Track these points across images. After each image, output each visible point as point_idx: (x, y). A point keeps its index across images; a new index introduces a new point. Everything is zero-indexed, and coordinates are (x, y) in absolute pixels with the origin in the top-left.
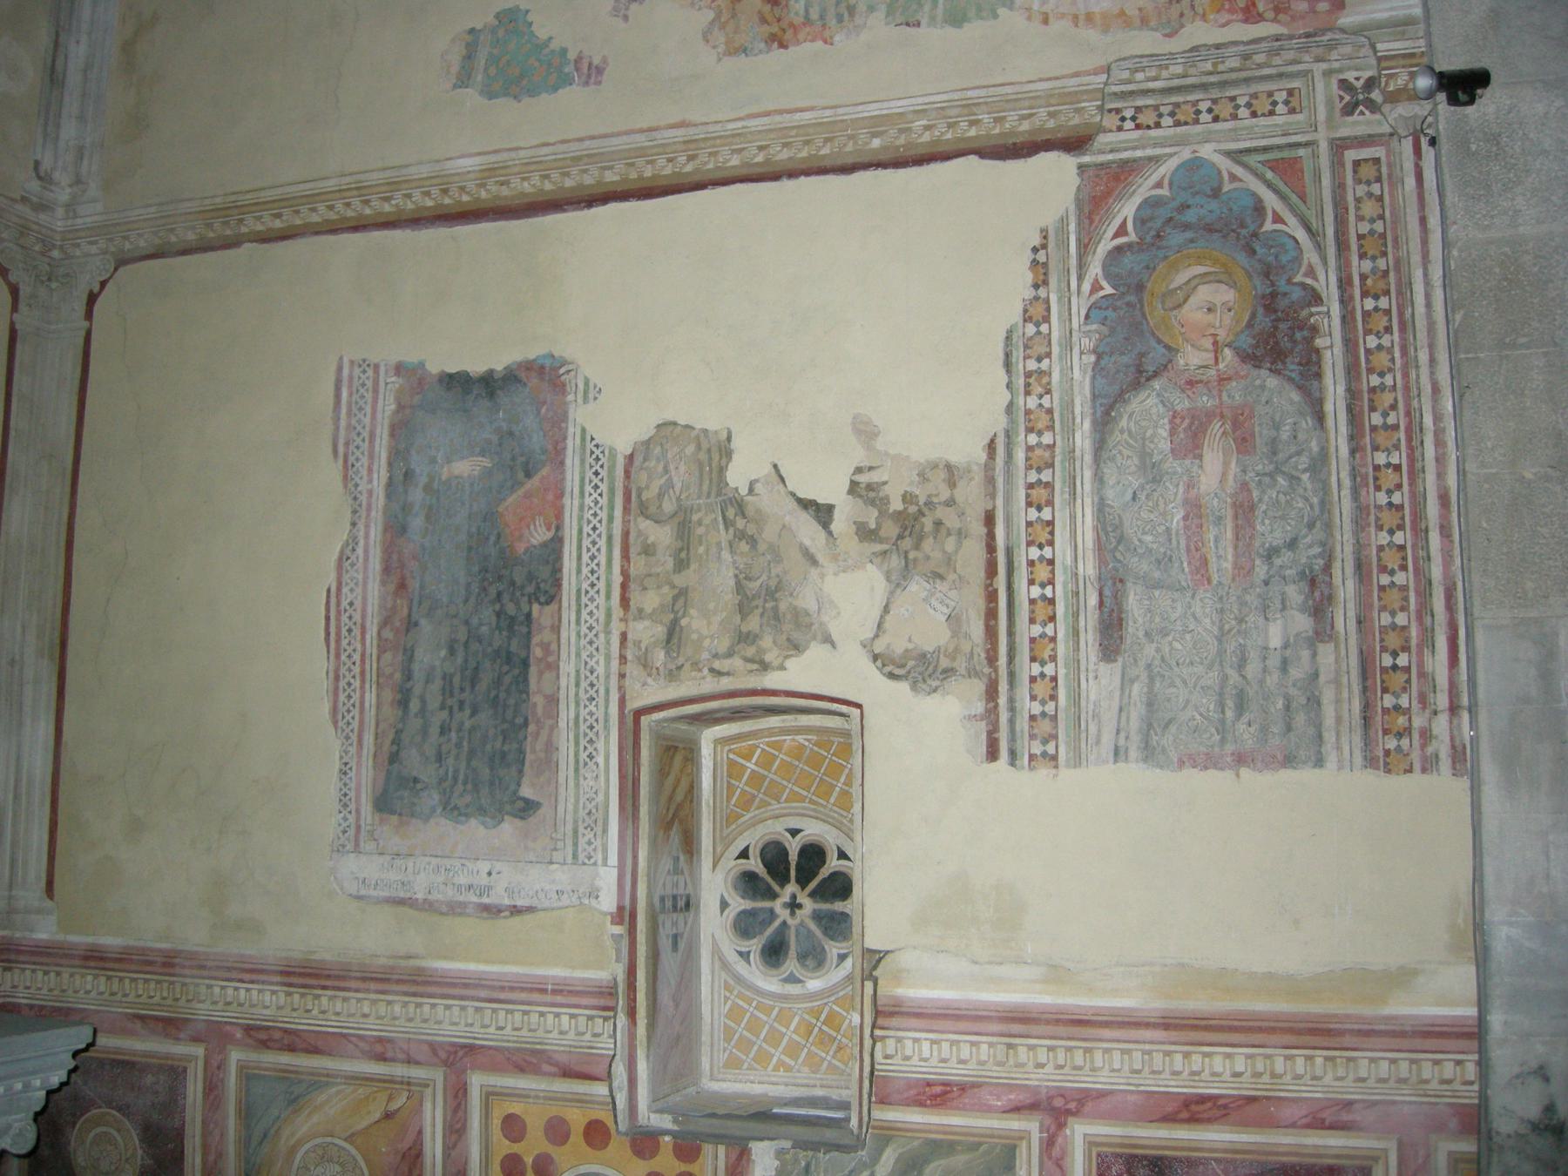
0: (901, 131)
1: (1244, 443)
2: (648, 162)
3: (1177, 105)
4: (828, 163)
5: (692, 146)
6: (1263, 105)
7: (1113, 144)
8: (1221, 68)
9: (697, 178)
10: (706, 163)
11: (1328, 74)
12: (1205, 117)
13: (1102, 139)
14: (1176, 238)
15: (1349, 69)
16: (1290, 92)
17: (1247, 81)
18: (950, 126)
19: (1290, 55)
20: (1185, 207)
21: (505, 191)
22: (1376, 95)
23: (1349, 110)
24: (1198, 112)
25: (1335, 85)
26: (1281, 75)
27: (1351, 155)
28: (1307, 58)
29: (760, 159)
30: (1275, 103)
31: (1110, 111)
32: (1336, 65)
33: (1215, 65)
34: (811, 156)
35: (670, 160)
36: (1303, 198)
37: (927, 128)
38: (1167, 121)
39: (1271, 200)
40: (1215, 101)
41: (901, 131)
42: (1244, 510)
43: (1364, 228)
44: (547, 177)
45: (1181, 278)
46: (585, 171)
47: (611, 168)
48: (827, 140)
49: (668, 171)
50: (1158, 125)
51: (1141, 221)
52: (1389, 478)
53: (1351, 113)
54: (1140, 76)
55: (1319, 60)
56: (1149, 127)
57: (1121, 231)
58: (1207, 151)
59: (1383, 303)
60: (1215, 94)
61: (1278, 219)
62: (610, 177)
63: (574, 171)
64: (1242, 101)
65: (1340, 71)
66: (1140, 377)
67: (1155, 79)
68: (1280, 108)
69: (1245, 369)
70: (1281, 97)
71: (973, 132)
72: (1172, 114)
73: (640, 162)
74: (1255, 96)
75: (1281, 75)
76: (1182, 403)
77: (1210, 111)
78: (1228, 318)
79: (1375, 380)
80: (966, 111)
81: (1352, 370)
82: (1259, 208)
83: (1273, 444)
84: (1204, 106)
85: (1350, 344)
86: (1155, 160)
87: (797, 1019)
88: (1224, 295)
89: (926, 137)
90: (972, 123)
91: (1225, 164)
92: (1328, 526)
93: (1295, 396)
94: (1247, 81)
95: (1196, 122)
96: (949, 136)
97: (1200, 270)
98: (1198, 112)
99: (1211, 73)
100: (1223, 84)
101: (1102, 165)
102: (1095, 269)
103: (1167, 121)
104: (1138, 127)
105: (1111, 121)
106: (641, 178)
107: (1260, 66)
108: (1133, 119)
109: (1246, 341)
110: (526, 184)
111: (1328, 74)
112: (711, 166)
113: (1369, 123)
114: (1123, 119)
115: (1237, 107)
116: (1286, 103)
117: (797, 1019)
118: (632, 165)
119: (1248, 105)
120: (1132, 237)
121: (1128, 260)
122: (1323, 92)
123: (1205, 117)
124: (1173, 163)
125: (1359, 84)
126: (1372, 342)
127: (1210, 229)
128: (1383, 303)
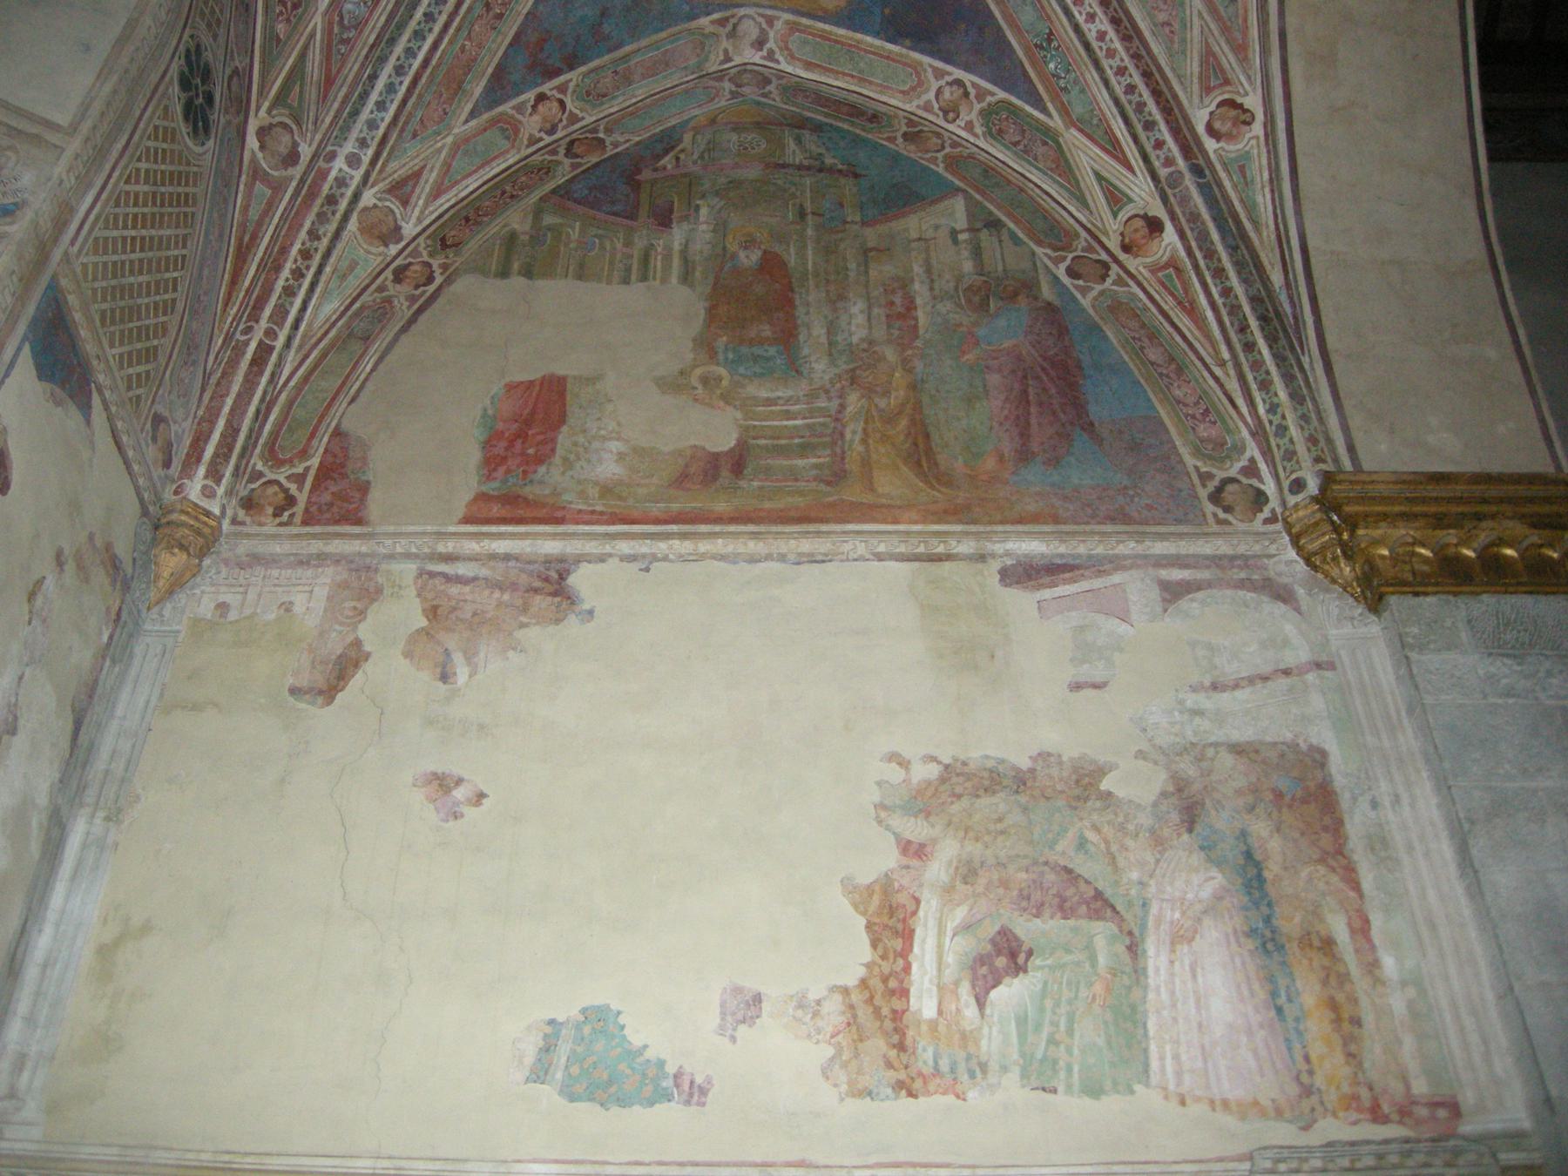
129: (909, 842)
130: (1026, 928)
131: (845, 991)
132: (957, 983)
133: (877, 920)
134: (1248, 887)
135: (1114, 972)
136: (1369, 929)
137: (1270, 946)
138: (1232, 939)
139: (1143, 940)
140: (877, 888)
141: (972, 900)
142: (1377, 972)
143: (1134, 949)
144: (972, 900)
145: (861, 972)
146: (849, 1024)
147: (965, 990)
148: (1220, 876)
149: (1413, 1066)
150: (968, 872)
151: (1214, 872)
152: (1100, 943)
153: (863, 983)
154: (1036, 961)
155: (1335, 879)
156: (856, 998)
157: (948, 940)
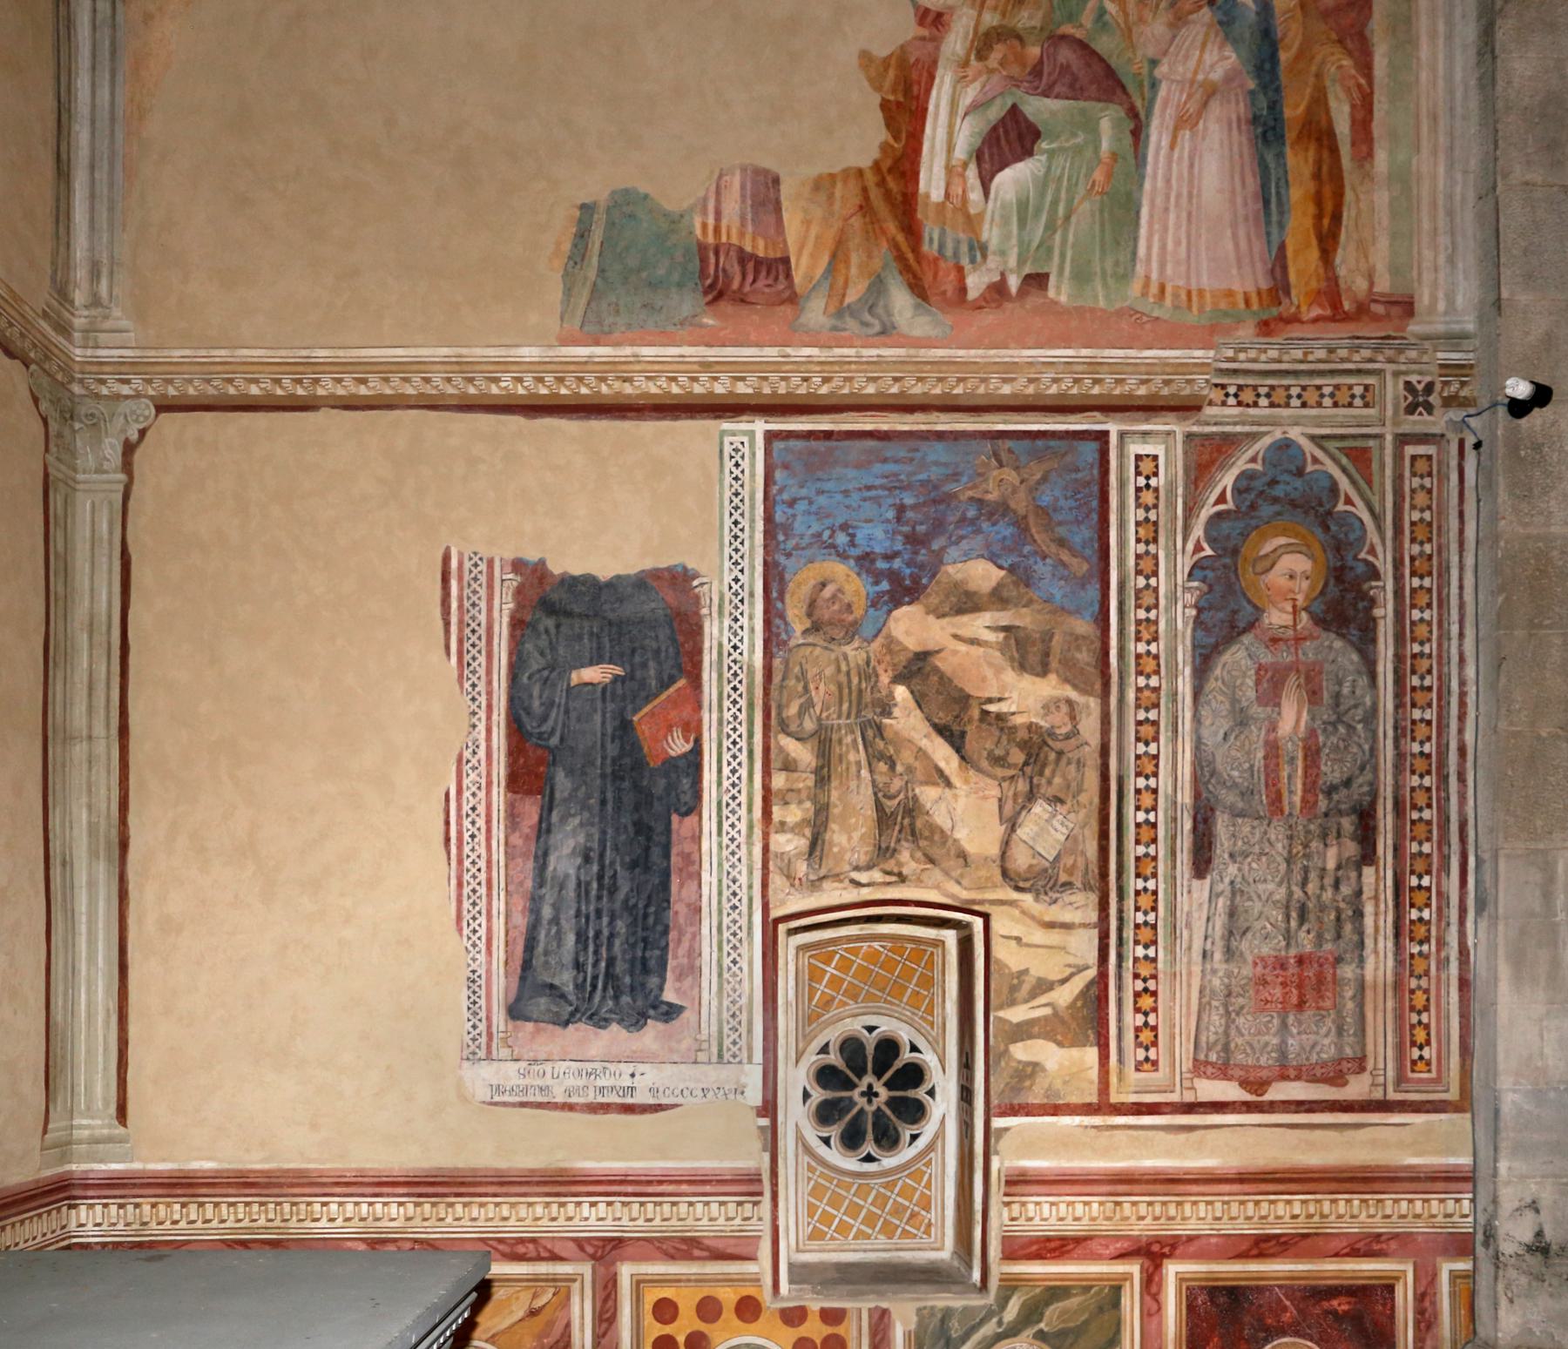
0: (1031, 381)
1: (1314, 696)
2: (783, 379)
3: (1272, 388)
4: (962, 402)
5: (827, 368)
6: (1343, 397)
7: (1221, 416)
8: (1310, 358)
9: (833, 401)
10: (841, 387)
11: (1396, 374)
12: (1295, 402)
13: (1209, 411)
14: (1266, 510)
15: (1413, 372)
16: (1367, 388)
17: (1332, 372)
18: (1076, 381)
19: (1366, 353)
20: (1273, 483)
21: (628, 389)
22: (1434, 399)
23: (1411, 409)
24: (1289, 397)
25: (1401, 386)
26: (1359, 372)
27: (1410, 450)
28: (1381, 358)
29: (894, 390)
30: (1353, 396)
31: (1216, 385)
32: (1403, 367)
33: (1305, 354)
34: (945, 394)
35: (805, 379)
36: (1369, 483)
37: (1055, 381)
38: (1263, 402)
39: (1344, 484)
40: (1304, 388)
41: (1031, 381)
42: (1312, 755)
43: (1416, 516)
44: (674, 379)
45: (1268, 548)
46: (716, 379)
47: (743, 379)
48: (960, 380)
49: (802, 391)
50: (1256, 404)
51: (1238, 491)
52: (1422, 730)
53: (1412, 413)
54: (1242, 356)
55: (1390, 361)
56: (1248, 405)
57: (1221, 499)
58: (1295, 433)
59: (1427, 582)
60: (1305, 381)
61: (1349, 501)
62: (742, 388)
63: (704, 377)
64: (1327, 390)
65: (1405, 373)
66: (1233, 631)
67: (1254, 361)
68: (1358, 402)
69: (1317, 631)
70: (1358, 390)
71: (1096, 390)
72: (1268, 396)
73: (774, 377)
74: (1337, 387)
75: (1359, 372)
76: (1266, 658)
77: (1299, 396)
78: (1305, 584)
79: (1416, 648)
80: (1091, 368)
81: (1399, 639)
82: (1334, 489)
83: (1337, 696)
84: (1295, 391)
85: (1399, 615)
86: (1254, 437)
87: (874, 1193)
88: (1300, 563)
89: (1054, 390)
90: (1096, 381)
91: (1308, 447)
92: (1375, 770)
93: (1355, 657)
94: (1332, 372)
95: (1288, 405)
96: (1075, 391)
97: (1282, 540)
98: (1289, 397)
99: (1302, 362)
100: (1311, 373)
101: (1208, 436)
102: (1198, 531)
103: (1263, 402)
104: (1239, 404)
105: (1217, 395)
106: (774, 394)
107: (1343, 360)
108: (1236, 395)
109: (1318, 608)
110: (651, 384)
111: (1396, 374)
112: (846, 391)
113: (1425, 423)
114: (1227, 395)
115: (1322, 396)
116: (1363, 397)
117: (874, 1193)
118: (766, 379)
119: (1332, 395)
120: (1230, 505)
121: (1226, 526)
122: (1393, 390)
123: (1295, 402)
124: (1267, 441)
125: (1420, 387)
126: (1416, 615)
127: (1293, 504)
128: (1427, 582)
129: (927, 11)
130: (1037, 108)
131: (860, 172)
132: (965, 165)
133: (891, 98)
134: (1259, 70)
135: (1114, 156)
136: (1371, 120)
137: (1270, 135)
138: (1234, 125)
139: (1148, 125)
140: (893, 62)
141: (984, 78)
142: (1367, 166)
143: (1138, 133)
144: (984, 78)
145: (875, 154)
146: (861, 207)
147: (972, 173)
148: (1234, 56)
149: (1381, 269)
150: (984, 44)
151: (1229, 52)
152: (1105, 125)
153: (877, 166)
154: (1044, 145)
155: (1347, 62)
156: (871, 179)
157: (959, 121)
